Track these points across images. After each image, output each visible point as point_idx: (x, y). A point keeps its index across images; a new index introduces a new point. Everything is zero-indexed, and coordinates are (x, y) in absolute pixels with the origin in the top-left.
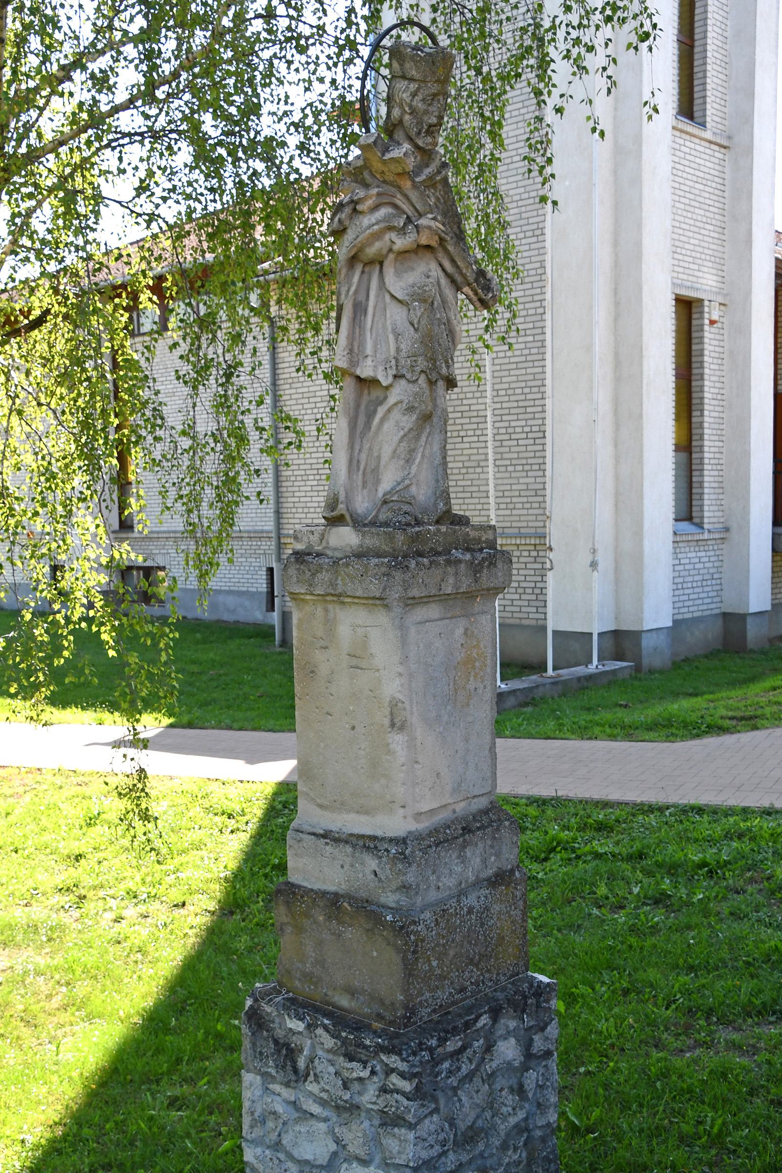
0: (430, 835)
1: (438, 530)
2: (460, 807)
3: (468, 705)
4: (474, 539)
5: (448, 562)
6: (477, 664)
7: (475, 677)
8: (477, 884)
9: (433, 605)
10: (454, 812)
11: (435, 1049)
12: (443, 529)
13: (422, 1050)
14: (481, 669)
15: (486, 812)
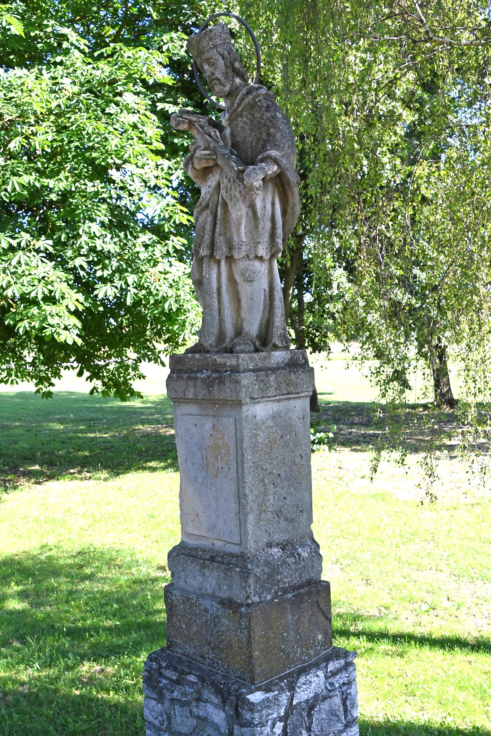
0: (189, 549)
1: (194, 357)
2: (218, 544)
3: (217, 476)
4: (220, 364)
5: (189, 378)
6: (222, 451)
7: (222, 459)
8: (213, 597)
9: (192, 405)
10: (213, 545)
11: (163, 668)
12: (197, 356)
13: (155, 662)
14: (225, 455)
15: (233, 556)
